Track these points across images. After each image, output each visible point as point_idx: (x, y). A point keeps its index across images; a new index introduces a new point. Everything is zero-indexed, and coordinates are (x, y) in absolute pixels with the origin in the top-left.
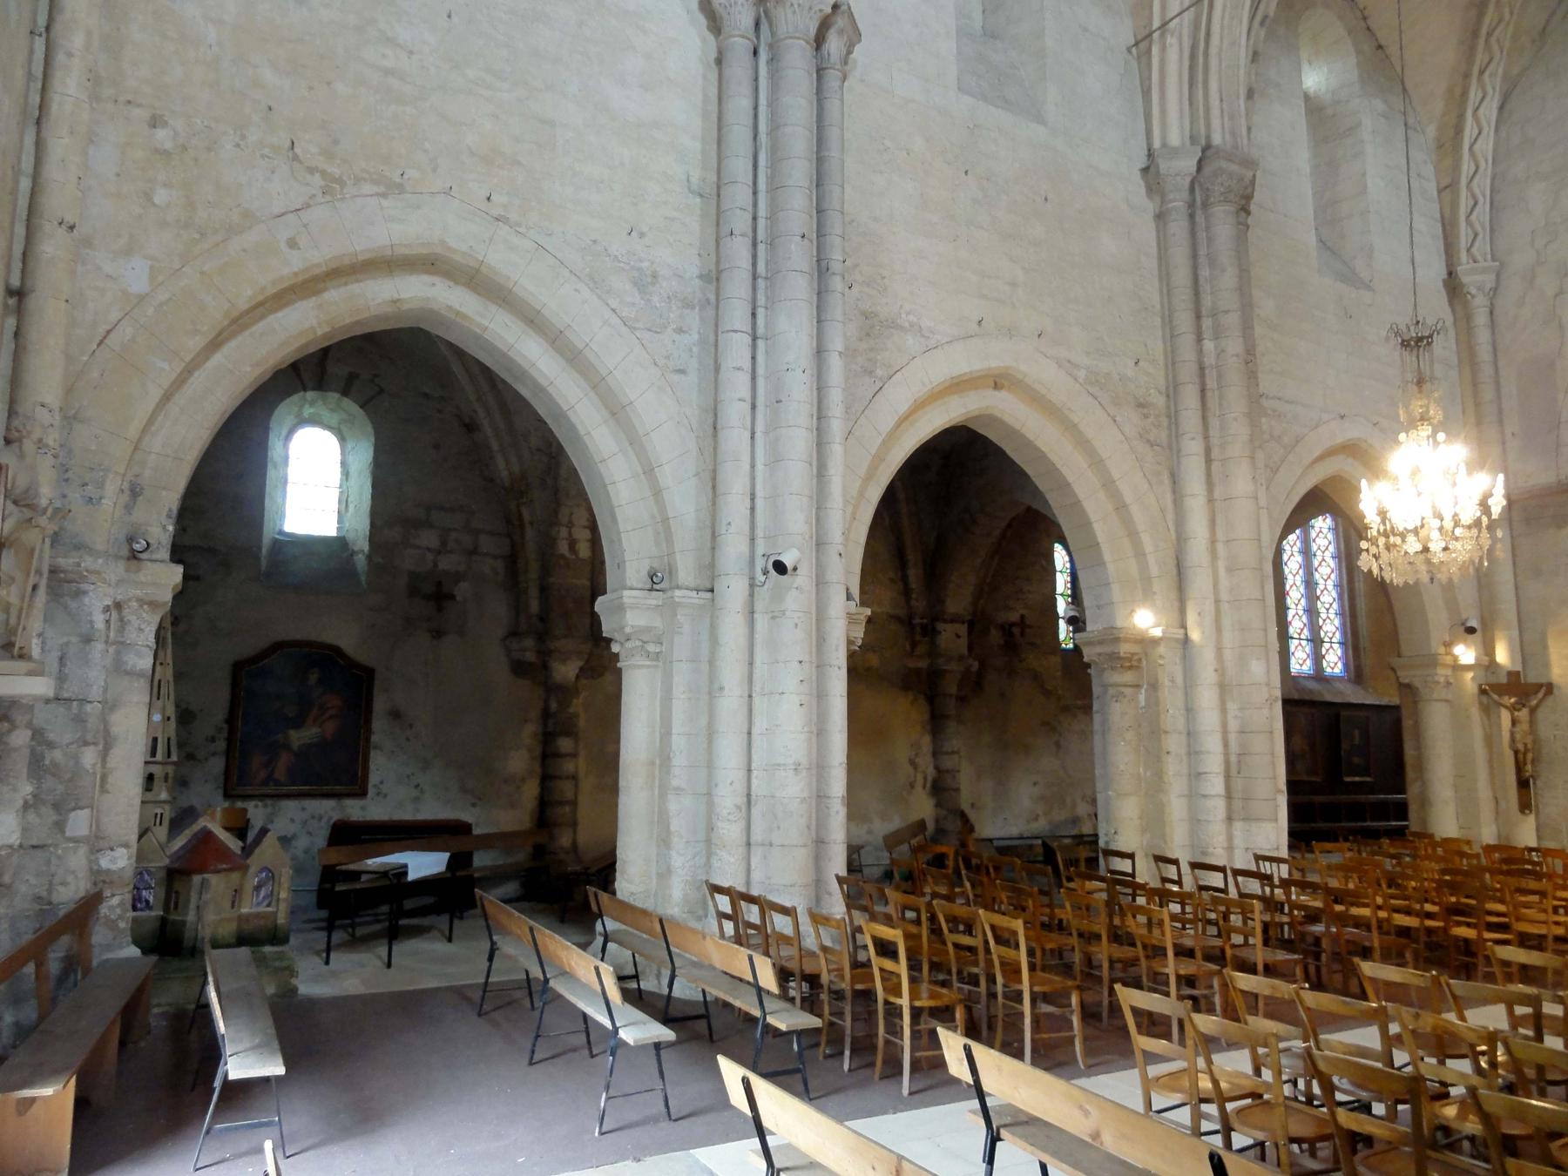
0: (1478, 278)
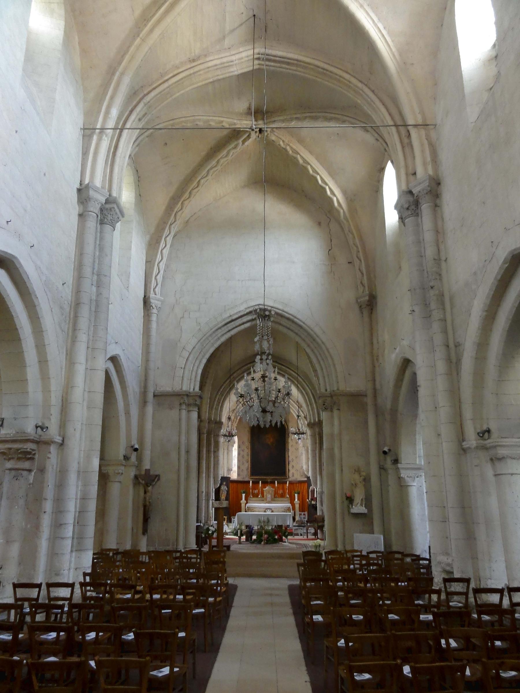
0: (156, 302)
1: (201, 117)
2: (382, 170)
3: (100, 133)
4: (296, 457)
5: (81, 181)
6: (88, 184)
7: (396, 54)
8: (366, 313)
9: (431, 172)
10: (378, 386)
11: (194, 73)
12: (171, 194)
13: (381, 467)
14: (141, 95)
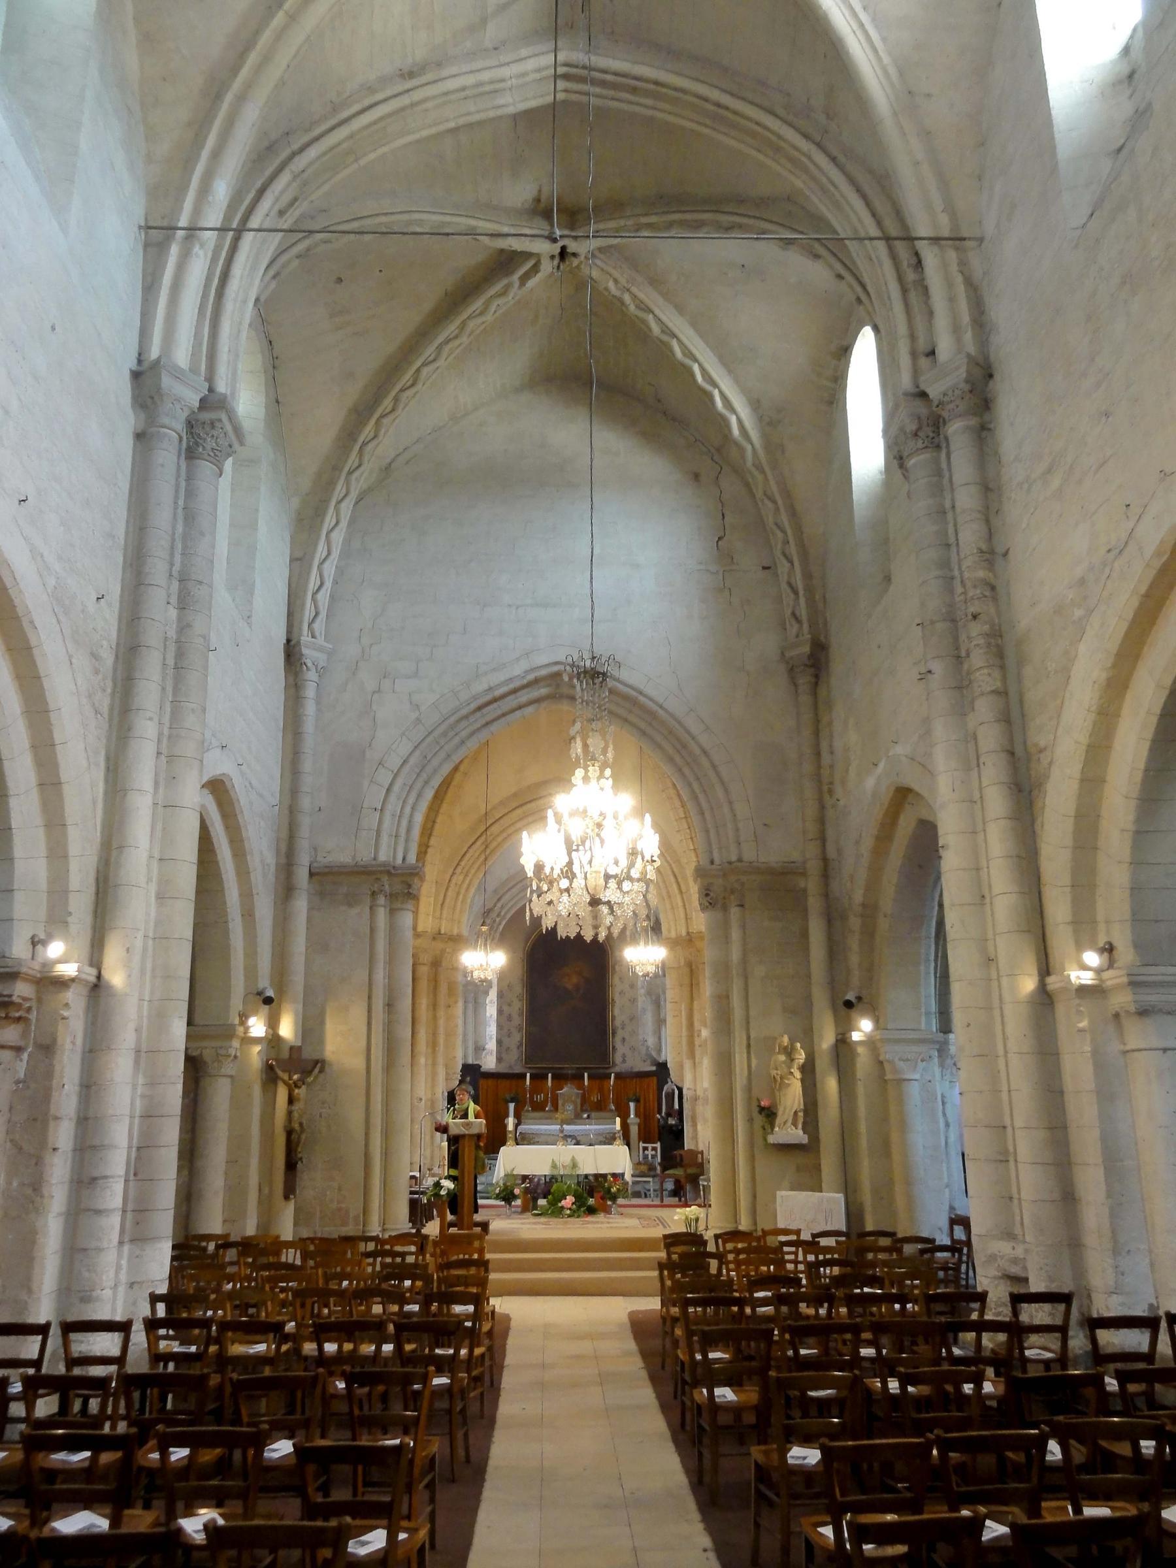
0: (316, 654)
1: (424, 216)
2: (844, 352)
3: (187, 238)
4: (631, 1020)
5: (140, 354)
6: (160, 357)
7: (892, 70)
8: (804, 681)
9: (971, 348)
10: (831, 853)
11: (413, 105)
14: (284, 155)
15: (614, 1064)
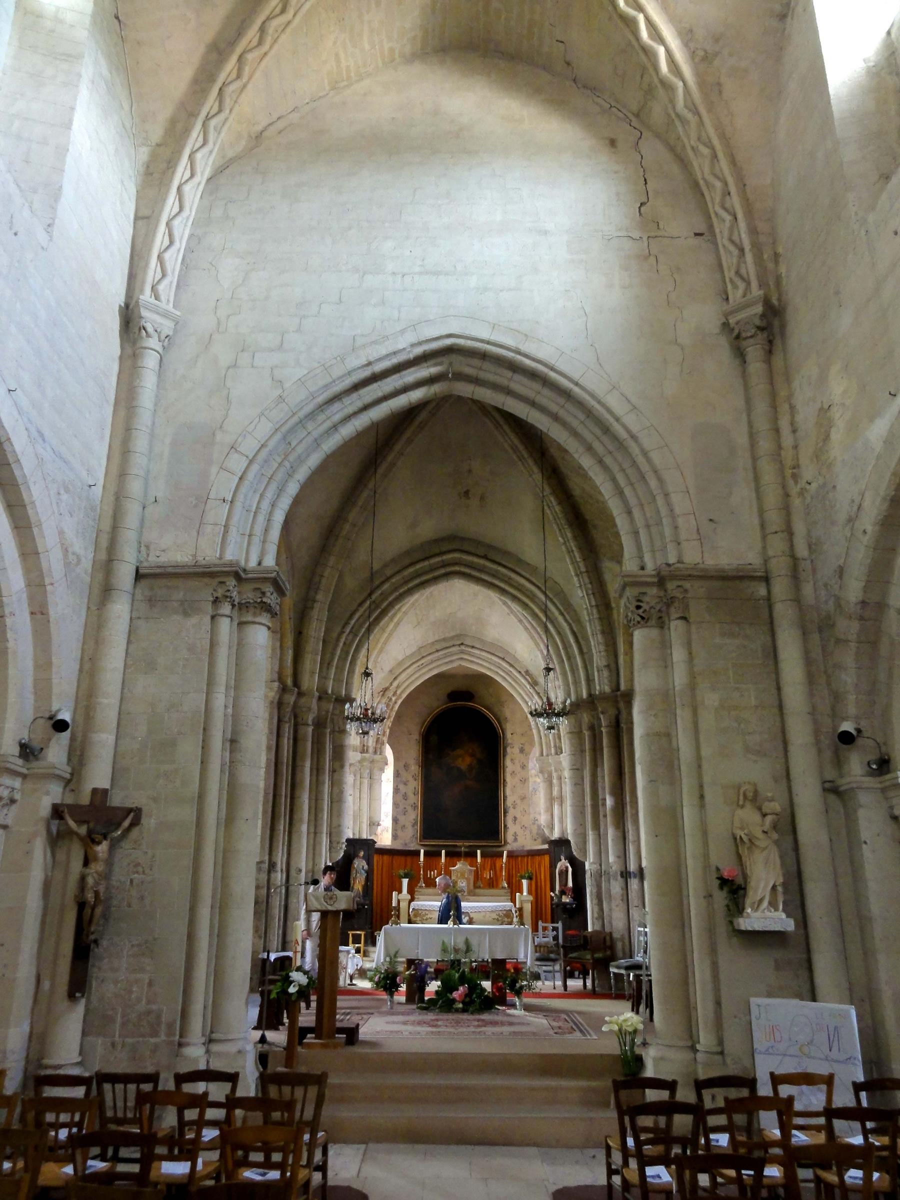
4: (523, 798)
10: (802, 550)
12: (209, 35)
13: (827, 785)
15: (506, 843)
